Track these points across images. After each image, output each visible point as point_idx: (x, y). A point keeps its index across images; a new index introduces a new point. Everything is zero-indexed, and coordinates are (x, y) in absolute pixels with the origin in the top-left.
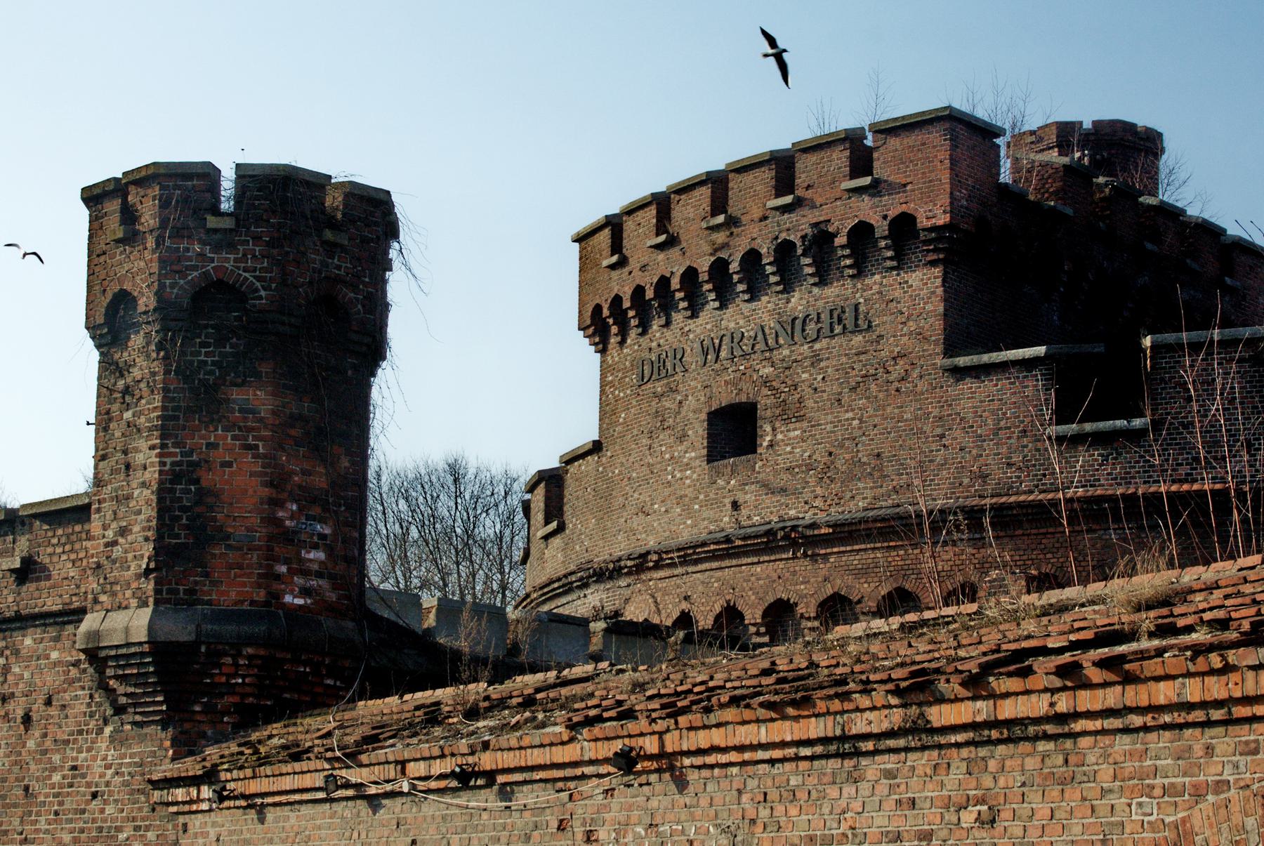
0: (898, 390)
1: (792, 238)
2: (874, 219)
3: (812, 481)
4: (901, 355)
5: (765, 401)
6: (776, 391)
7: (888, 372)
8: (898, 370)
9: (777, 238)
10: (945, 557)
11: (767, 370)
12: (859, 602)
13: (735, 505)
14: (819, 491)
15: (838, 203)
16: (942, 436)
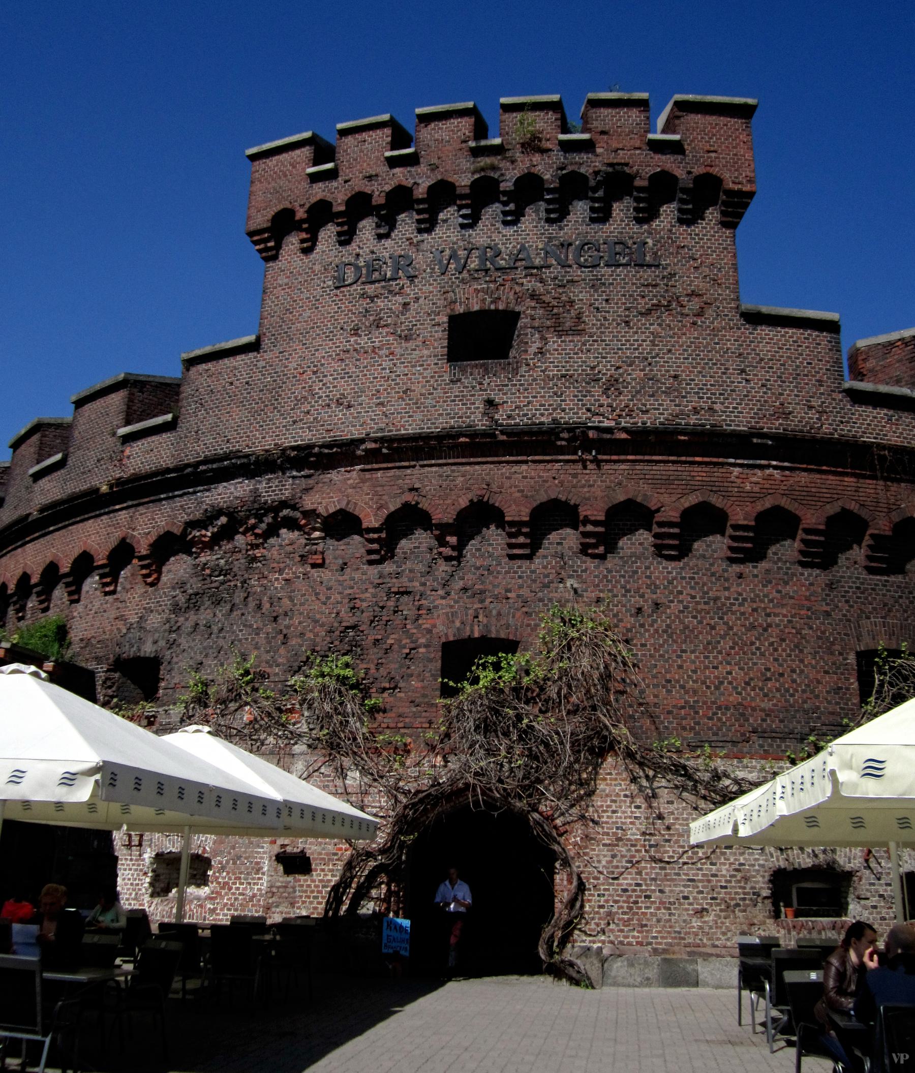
0: (694, 323)
1: (583, 170)
2: (680, 173)
3: (597, 390)
4: (693, 294)
5: (528, 310)
6: (546, 306)
7: (682, 306)
8: (694, 305)
9: (562, 169)
10: (754, 479)
11: (530, 284)
12: (658, 510)
13: (490, 403)
14: (604, 400)
15: (638, 152)
16: (743, 371)
